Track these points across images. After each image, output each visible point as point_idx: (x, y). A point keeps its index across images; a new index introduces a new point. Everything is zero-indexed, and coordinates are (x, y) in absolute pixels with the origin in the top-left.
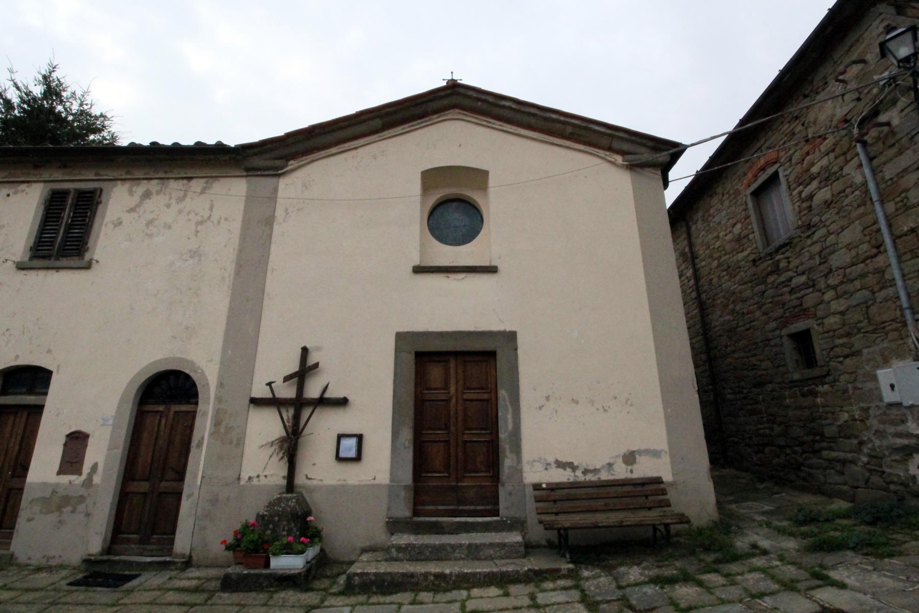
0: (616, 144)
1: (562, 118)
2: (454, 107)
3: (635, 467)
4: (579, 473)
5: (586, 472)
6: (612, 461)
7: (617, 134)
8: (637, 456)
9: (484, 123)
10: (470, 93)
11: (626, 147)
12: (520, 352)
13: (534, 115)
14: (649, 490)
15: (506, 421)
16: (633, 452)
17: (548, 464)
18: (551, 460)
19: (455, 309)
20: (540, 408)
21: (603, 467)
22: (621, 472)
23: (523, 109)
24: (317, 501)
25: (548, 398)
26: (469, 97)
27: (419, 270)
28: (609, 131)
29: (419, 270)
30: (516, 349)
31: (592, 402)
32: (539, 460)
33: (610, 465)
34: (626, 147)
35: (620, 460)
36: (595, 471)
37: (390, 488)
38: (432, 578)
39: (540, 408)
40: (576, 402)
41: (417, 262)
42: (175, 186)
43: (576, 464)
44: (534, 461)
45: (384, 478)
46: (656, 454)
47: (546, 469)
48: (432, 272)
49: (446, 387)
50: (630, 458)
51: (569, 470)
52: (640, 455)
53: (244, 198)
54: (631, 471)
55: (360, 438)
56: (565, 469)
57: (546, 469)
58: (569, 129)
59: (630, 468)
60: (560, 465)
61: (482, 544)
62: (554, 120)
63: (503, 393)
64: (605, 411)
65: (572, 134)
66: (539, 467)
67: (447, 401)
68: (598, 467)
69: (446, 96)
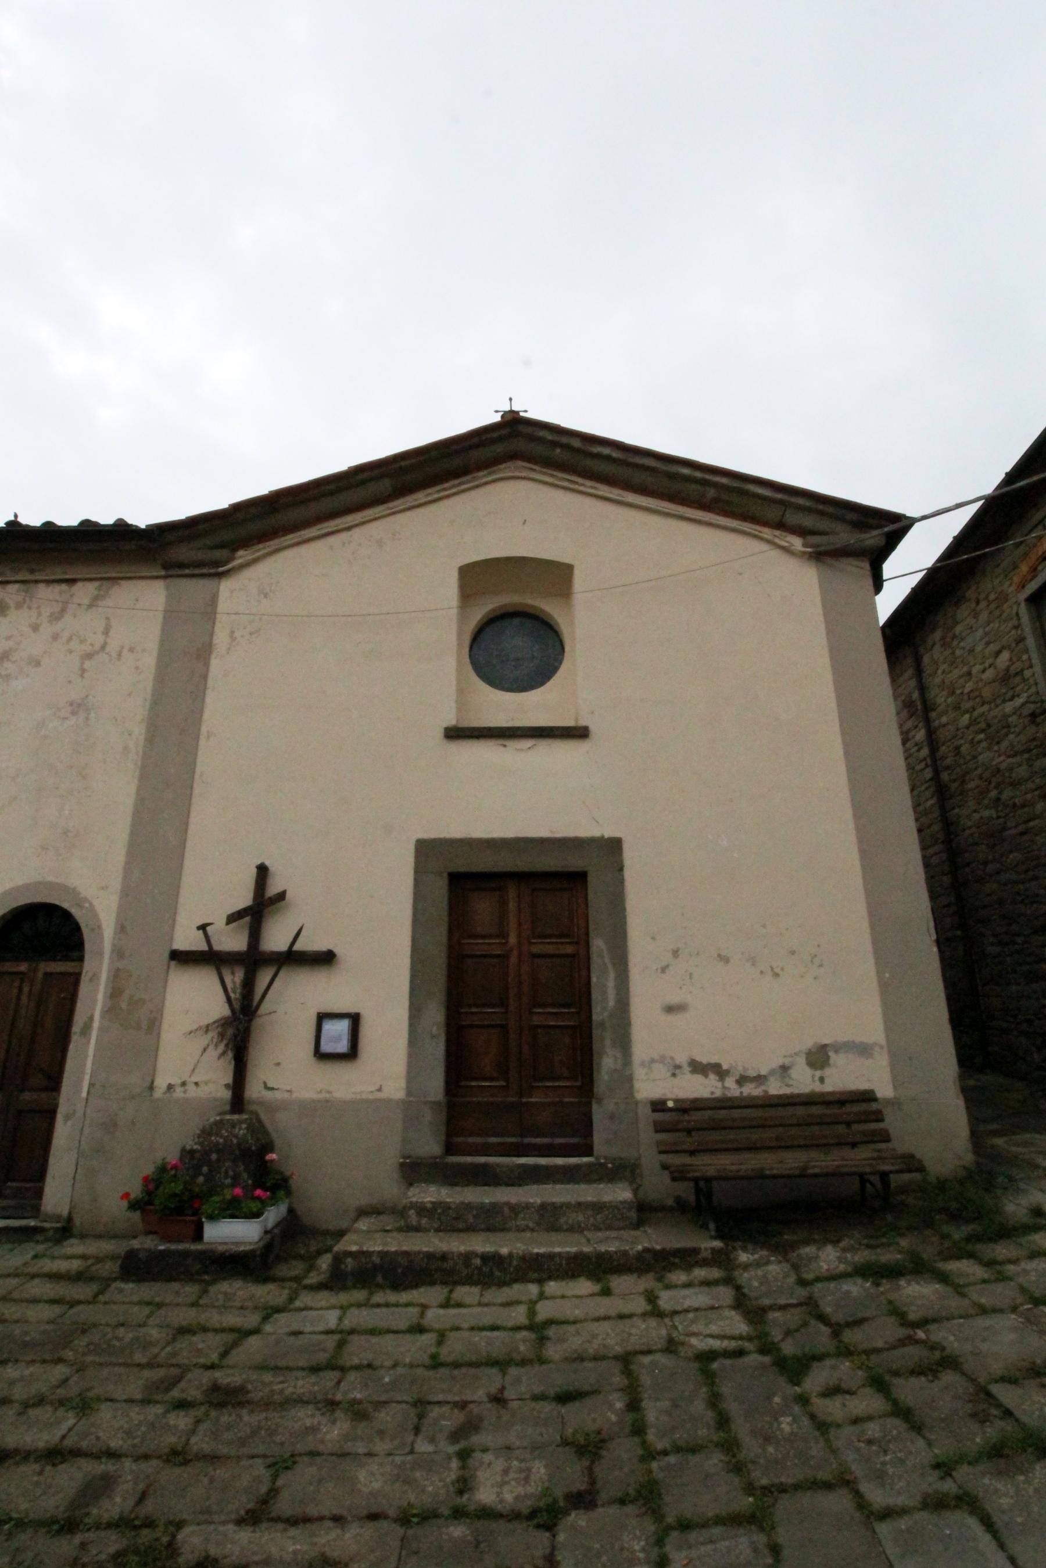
0: (793, 518)
1: (698, 474)
2: (513, 456)
3: (828, 1071)
4: (730, 1082)
5: (742, 1080)
6: (787, 1061)
7: (793, 500)
8: (831, 1054)
9: (566, 484)
10: (542, 433)
11: (808, 521)
12: (627, 873)
13: (653, 470)
14: (852, 1115)
15: (604, 992)
16: (824, 1047)
17: (678, 1067)
18: (682, 1059)
19: (517, 799)
20: (664, 970)
21: (772, 1072)
22: (803, 1081)
24: (283, 1127)
25: (676, 953)
26: (542, 440)
27: (455, 734)
28: (779, 496)
29: (455, 734)
30: (621, 869)
31: (753, 961)
32: (662, 1059)
33: (784, 1069)
34: (808, 521)
35: (801, 1061)
36: (760, 1079)
37: (405, 1104)
39: (664, 970)
40: (724, 959)
41: (451, 720)
42: (45, 593)
43: (725, 1067)
44: (653, 1061)
45: (395, 1089)
46: (863, 1050)
47: (674, 1075)
48: (478, 737)
49: (503, 934)
50: (819, 1057)
51: (713, 1077)
52: (836, 1052)
53: (160, 616)
54: (822, 1080)
55: (355, 1020)
56: (706, 1076)
57: (674, 1075)
58: (711, 493)
59: (818, 1073)
60: (699, 1068)
61: (563, 1205)
62: (687, 479)
63: (598, 944)
64: (776, 975)
65: (716, 500)
66: (661, 1071)
67: (504, 957)
68: (763, 1073)
69: (500, 439)
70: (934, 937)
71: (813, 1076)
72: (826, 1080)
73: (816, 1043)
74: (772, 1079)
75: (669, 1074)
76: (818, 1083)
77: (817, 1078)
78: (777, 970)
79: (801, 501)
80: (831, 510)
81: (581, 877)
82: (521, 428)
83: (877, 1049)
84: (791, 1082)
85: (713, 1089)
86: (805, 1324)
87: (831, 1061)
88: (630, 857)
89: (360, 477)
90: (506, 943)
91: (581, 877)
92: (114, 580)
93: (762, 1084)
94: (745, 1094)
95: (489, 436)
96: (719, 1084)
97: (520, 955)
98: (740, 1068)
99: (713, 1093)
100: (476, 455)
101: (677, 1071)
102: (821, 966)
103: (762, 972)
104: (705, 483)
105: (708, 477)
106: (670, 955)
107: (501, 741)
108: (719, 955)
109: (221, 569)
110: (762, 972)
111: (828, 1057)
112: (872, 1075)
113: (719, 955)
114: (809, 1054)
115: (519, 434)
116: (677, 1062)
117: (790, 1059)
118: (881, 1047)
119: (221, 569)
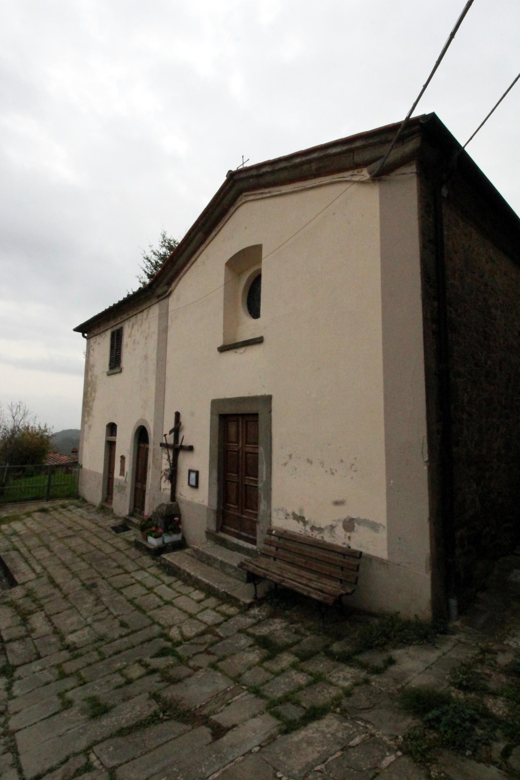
0: (358, 158)
1: (304, 159)
2: (240, 192)
3: (353, 535)
4: (308, 528)
5: (313, 528)
6: (334, 523)
7: (353, 146)
8: (356, 525)
9: (260, 196)
10: (243, 175)
11: (367, 155)
12: (273, 414)
13: (285, 168)
14: (350, 564)
15: (262, 474)
16: (353, 519)
17: (288, 515)
18: (290, 511)
19: (241, 378)
20: (285, 464)
21: (326, 527)
22: (339, 538)
23: (277, 167)
24: (183, 508)
25: (290, 456)
26: (243, 179)
27: (223, 349)
28: (345, 148)
29: (223, 349)
30: (270, 412)
31: (322, 463)
32: (282, 509)
33: (332, 527)
34: (367, 155)
35: (341, 525)
36: (321, 530)
37: (208, 509)
38: (186, 574)
39: (285, 464)
40: (310, 462)
41: (220, 344)
42: (139, 316)
43: (306, 519)
44: (279, 510)
45: (206, 503)
46: (374, 526)
47: (286, 518)
48: (228, 350)
49: (238, 442)
50: (349, 525)
51: (301, 523)
52: (359, 524)
53: (157, 318)
54: (349, 538)
55: (197, 473)
56: (299, 522)
57: (286, 518)
58: (314, 166)
59: (348, 534)
60: (300, 519)
61: (227, 564)
62: (302, 164)
63: (261, 450)
64: (332, 473)
65: (317, 170)
66: (282, 515)
67: (238, 452)
68: (322, 527)
69: (231, 188)
70: (427, 459)
71: (345, 535)
72: (352, 539)
73: (348, 517)
74: (326, 531)
75: (284, 517)
76: (347, 539)
77: (347, 537)
78: (333, 471)
79: (358, 144)
80: (376, 140)
81: (256, 415)
82: (236, 177)
83: (381, 528)
84: (335, 536)
85: (301, 530)
86: (10, 641)
87: (355, 529)
88: (275, 404)
89: (191, 236)
90: (238, 446)
91: (256, 415)
92: (149, 307)
93: (321, 533)
94: (314, 537)
95: (225, 190)
96: (303, 527)
97: (242, 452)
98: (312, 521)
99: (301, 531)
100: (225, 202)
101: (288, 517)
102: (355, 471)
103: (326, 471)
104: (310, 162)
105: (308, 157)
106: (288, 457)
107: (235, 350)
108: (308, 460)
109: (167, 294)
110: (326, 471)
111: (354, 526)
112: (372, 543)
113: (308, 460)
114: (345, 522)
115: (235, 182)
116: (288, 512)
117: (335, 522)
118: (384, 527)
119: (167, 294)
